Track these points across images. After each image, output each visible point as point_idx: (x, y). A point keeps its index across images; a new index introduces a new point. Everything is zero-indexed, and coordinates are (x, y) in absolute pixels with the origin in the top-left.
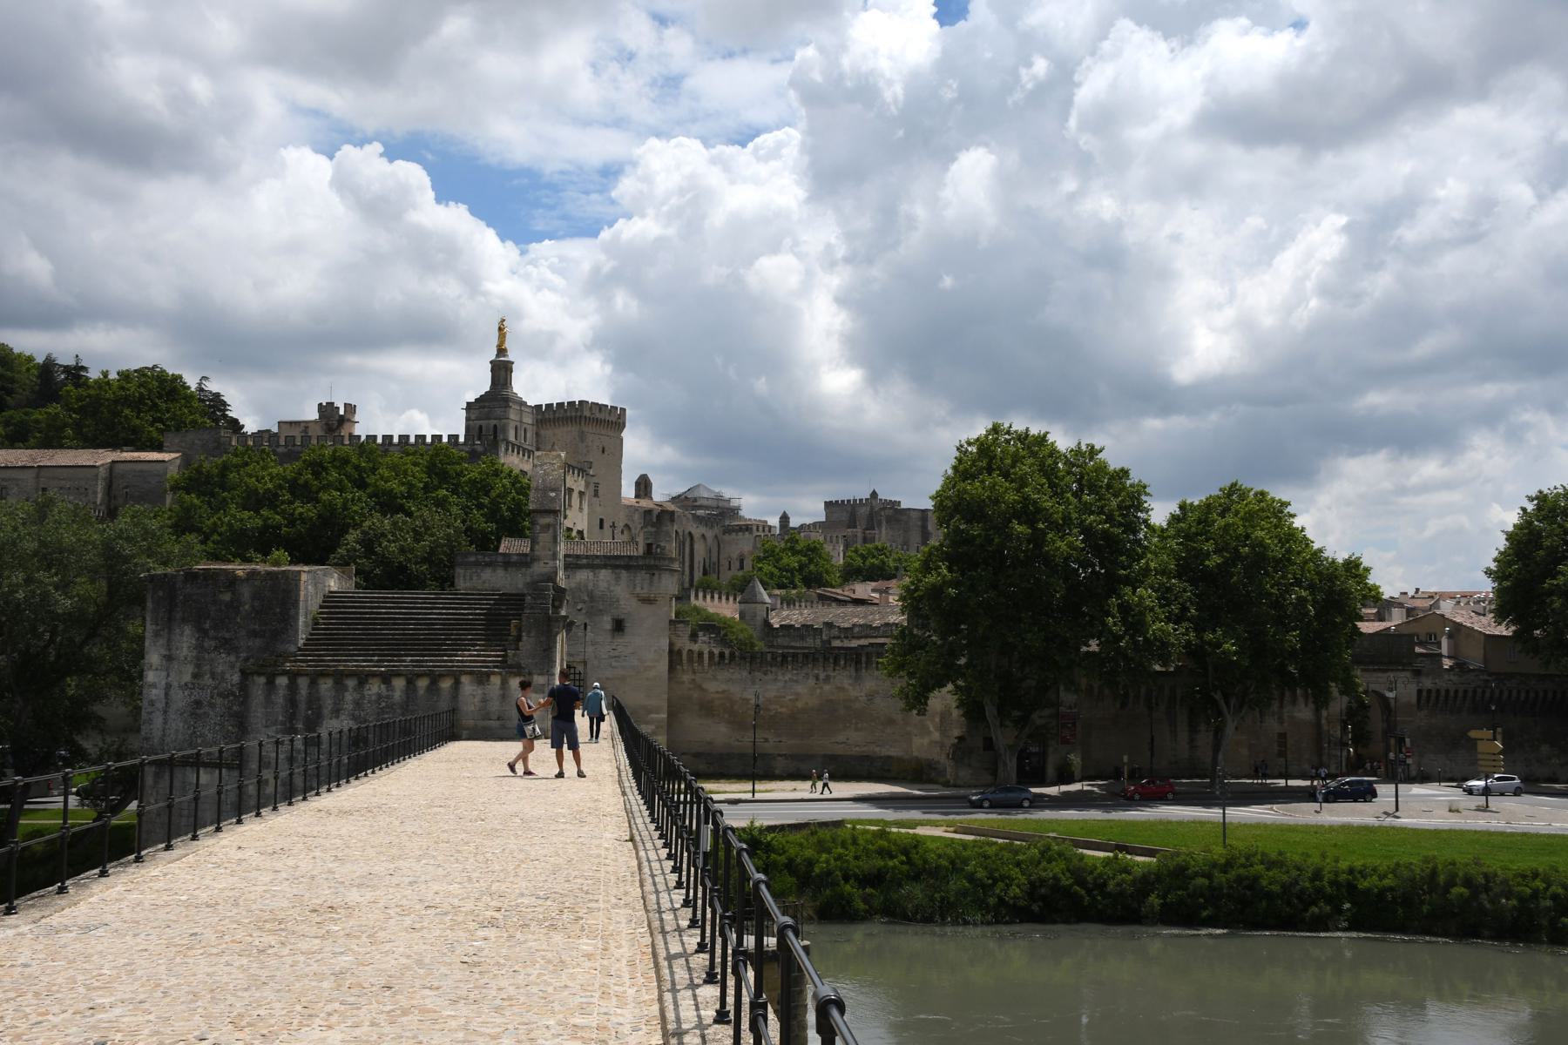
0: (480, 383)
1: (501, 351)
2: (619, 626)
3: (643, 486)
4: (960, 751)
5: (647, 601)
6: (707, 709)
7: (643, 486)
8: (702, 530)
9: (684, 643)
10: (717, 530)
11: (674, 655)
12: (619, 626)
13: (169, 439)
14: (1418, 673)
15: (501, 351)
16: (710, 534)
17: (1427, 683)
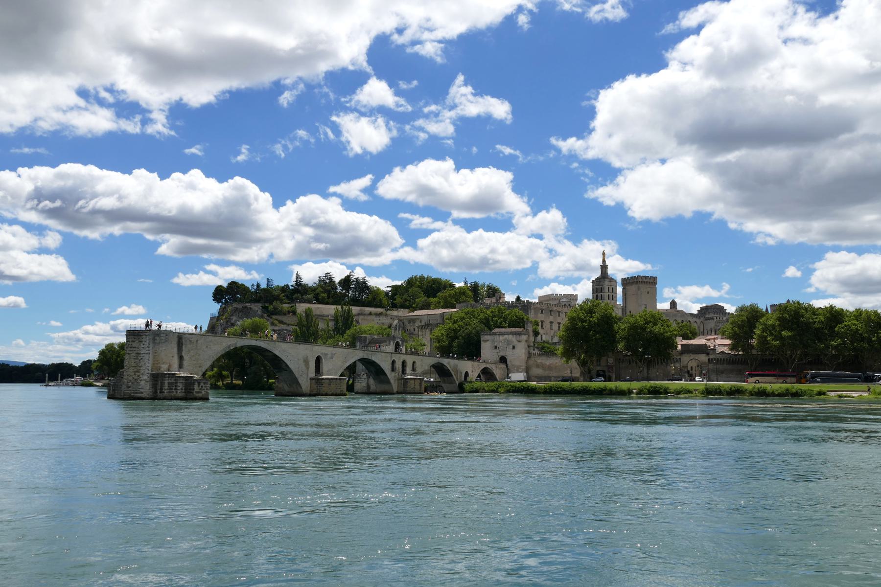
0: (597, 274)
1: (604, 261)
2: (514, 347)
3: (673, 304)
4: (582, 373)
5: (519, 341)
6: (538, 366)
7: (673, 304)
8: (695, 319)
9: (532, 351)
10: (702, 319)
11: (530, 356)
12: (514, 347)
13: (457, 305)
14: (708, 354)
15: (604, 261)
16: (698, 321)
17: (711, 357)
